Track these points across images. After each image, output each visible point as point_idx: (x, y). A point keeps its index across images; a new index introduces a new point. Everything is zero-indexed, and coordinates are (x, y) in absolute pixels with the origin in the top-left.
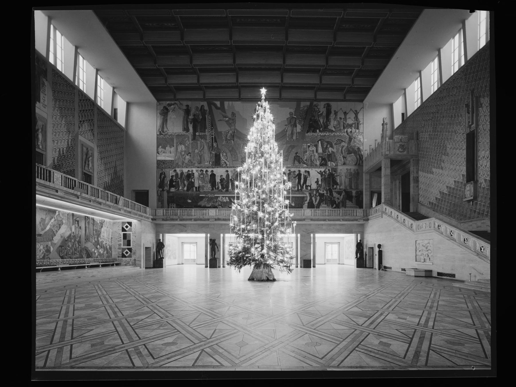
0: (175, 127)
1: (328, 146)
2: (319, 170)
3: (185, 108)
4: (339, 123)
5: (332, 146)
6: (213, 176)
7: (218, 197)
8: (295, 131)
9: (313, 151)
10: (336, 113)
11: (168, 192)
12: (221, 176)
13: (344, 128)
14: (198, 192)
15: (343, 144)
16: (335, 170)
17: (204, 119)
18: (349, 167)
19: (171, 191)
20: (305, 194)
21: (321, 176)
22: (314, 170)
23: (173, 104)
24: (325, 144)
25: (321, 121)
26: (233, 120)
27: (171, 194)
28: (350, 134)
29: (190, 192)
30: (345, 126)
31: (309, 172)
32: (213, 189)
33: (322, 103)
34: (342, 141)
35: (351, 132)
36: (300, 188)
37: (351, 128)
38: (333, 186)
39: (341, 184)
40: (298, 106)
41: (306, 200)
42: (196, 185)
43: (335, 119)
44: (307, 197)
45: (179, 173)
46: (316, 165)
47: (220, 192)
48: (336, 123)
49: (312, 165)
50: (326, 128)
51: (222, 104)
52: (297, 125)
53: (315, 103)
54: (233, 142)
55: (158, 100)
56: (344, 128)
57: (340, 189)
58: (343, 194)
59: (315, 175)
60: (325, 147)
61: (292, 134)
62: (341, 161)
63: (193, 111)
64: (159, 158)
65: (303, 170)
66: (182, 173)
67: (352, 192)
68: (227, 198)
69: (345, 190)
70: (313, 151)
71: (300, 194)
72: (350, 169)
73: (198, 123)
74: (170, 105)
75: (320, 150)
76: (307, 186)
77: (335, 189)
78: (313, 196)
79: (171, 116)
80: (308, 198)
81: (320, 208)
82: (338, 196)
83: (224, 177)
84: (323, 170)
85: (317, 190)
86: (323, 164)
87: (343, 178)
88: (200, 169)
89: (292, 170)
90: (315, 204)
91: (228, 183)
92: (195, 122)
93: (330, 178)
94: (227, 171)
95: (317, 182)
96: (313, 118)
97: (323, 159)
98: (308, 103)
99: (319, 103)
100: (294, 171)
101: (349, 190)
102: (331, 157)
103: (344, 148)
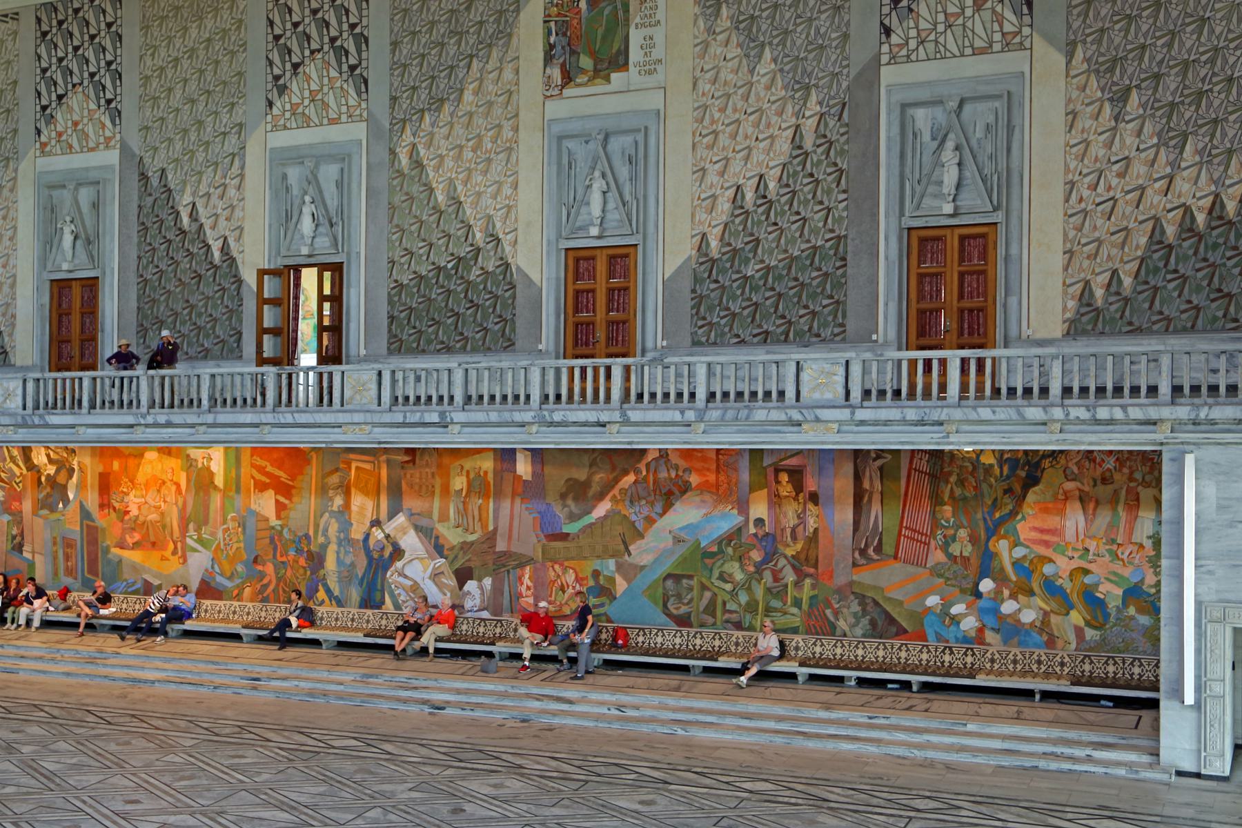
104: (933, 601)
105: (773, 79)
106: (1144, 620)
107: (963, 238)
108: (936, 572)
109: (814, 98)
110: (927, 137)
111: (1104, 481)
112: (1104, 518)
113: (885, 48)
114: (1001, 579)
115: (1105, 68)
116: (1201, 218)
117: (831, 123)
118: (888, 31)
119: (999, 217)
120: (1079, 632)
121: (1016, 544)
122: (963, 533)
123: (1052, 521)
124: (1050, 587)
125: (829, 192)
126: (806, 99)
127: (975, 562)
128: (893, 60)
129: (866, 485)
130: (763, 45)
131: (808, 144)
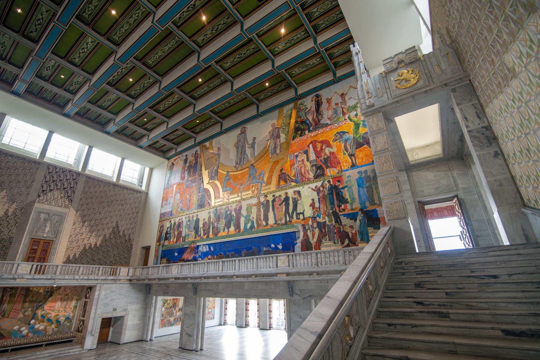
0: (176, 179)
1: (324, 147)
2: (313, 186)
3: (185, 158)
4: (336, 112)
5: (329, 146)
6: (198, 221)
7: (198, 247)
8: (278, 143)
9: (303, 160)
10: (329, 101)
11: (163, 246)
12: (204, 219)
13: (344, 114)
14: (184, 243)
15: (346, 136)
16: (339, 179)
17: (196, 163)
18: (363, 169)
19: (165, 244)
20: (297, 227)
21: (318, 194)
22: (306, 187)
23: (177, 159)
24: (319, 146)
25: (310, 118)
26: (218, 154)
27: (164, 249)
28: (355, 119)
29: (178, 244)
30: (345, 111)
31: (299, 193)
32: (196, 238)
33: (308, 97)
34: (344, 133)
35: (356, 115)
36: (288, 219)
37: (356, 111)
38: (339, 206)
39: (353, 199)
40: (280, 114)
41: (299, 238)
42: (183, 235)
43: (328, 109)
44: (299, 231)
45: (173, 222)
46: (309, 179)
47: (202, 240)
48: (330, 112)
49: (302, 180)
50: (317, 125)
51: (211, 144)
52: (281, 135)
53: (299, 102)
54: (216, 177)
55: (168, 159)
56: (344, 114)
57: (352, 209)
58: (360, 217)
59: (308, 194)
60: (319, 149)
61: (275, 148)
62: (347, 162)
63: (190, 158)
64: (163, 212)
65: (290, 192)
66: (175, 223)
67: (375, 211)
68: (207, 246)
69: (361, 210)
70: (303, 160)
71: (288, 229)
72: (366, 171)
73: (193, 168)
74: (175, 160)
75: (313, 156)
76: (298, 214)
77: (344, 210)
78: (309, 229)
79: (175, 168)
80: (302, 234)
81: (323, 249)
82: (351, 222)
83: (207, 220)
84: (319, 184)
85: (314, 218)
86: (320, 173)
87: (355, 188)
88: (188, 216)
89: (277, 194)
90: (312, 242)
91: (209, 228)
92: (190, 167)
93: (332, 194)
94: (209, 213)
95: (312, 205)
96: (299, 120)
97: (319, 168)
98: (292, 105)
99: (305, 99)
100: (280, 196)
101: (370, 208)
102: (331, 161)
103: (348, 144)
104: (16, 328)
105: (4, 197)
106: (68, 324)
107: (44, 242)
108: (20, 320)
109: (15, 204)
110: (42, 220)
111: (67, 295)
112: (65, 303)
113: (38, 199)
114: (37, 319)
115: (83, 216)
116: (93, 246)
117: (18, 211)
118: (39, 196)
119: (54, 239)
120: (53, 329)
121: (43, 310)
122: (30, 309)
123: (53, 304)
124: (49, 320)
125: (12, 226)
126: (13, 204)
127: (31, 316)
128: (39, 202)
129: (5, 299)
130: (4, 189)
131: (10, 214)
